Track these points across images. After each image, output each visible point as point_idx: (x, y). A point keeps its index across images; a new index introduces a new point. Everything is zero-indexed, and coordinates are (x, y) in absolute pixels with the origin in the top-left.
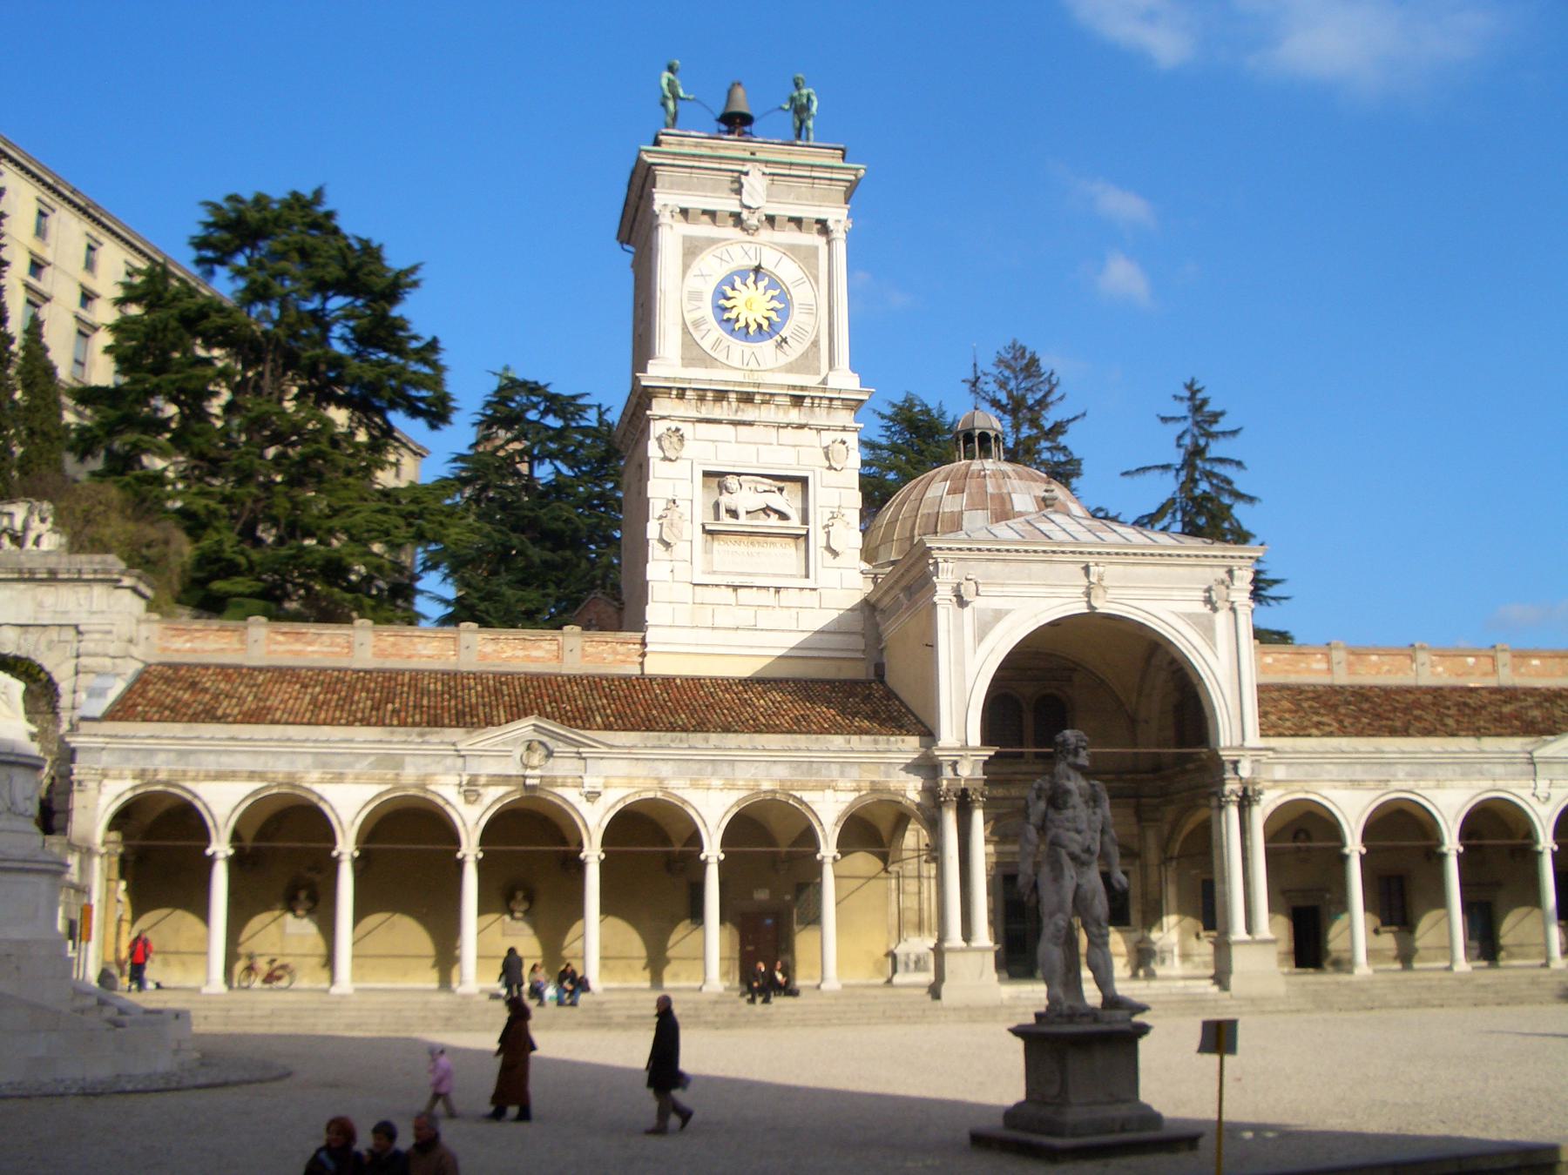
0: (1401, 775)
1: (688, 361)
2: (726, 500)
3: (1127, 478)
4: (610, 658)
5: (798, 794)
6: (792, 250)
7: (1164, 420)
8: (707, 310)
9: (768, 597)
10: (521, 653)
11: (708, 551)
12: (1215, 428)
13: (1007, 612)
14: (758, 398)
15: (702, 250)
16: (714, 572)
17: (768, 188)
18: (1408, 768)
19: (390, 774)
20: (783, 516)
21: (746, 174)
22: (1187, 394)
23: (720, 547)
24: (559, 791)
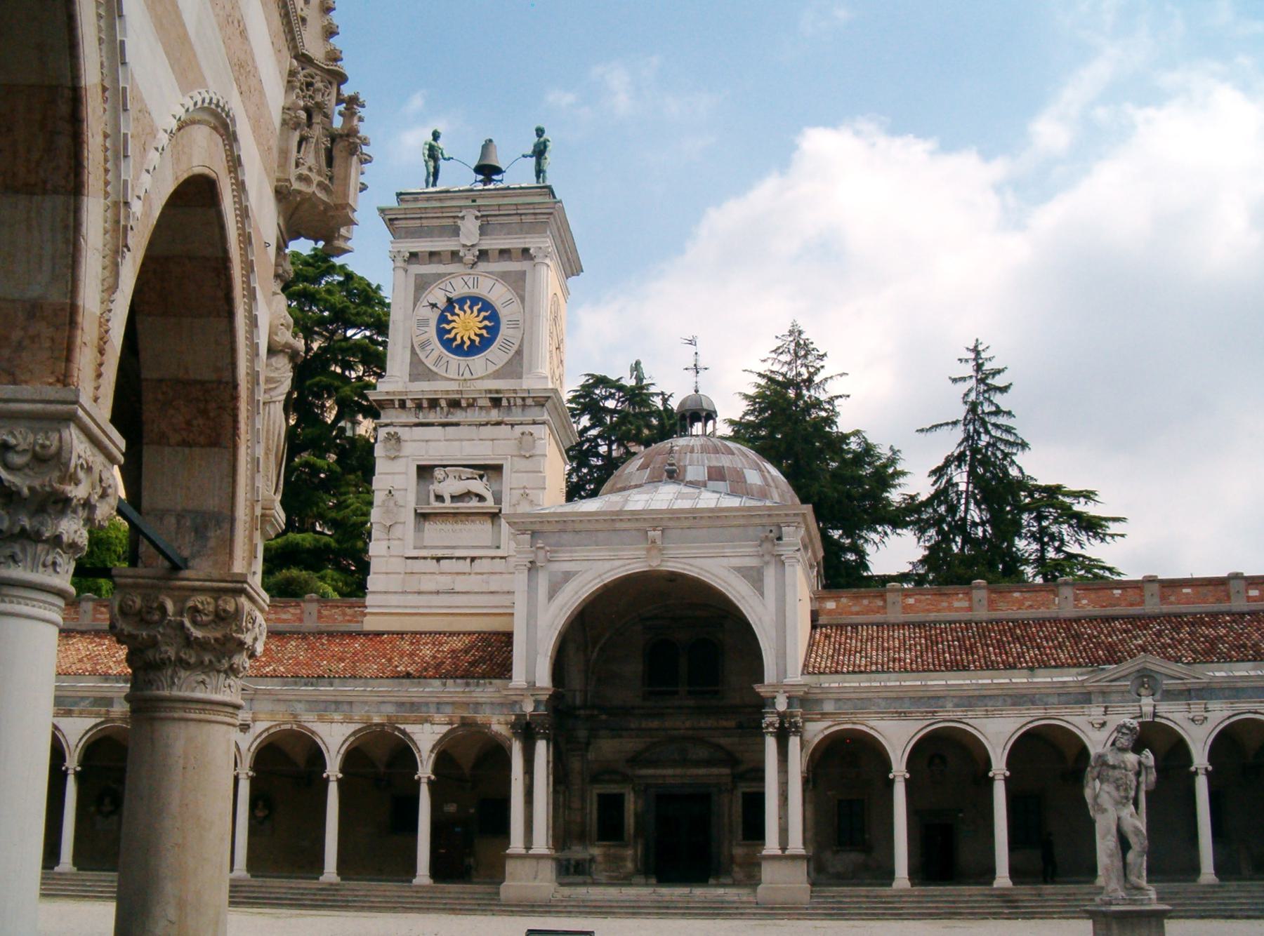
0: (949, 706)
1: (414, 377)
2: (436, 487)
3: (923, 435)
4: (340, 618)
5: (402, 727)
6: (504, 276)
7: (955, 380)
9: (464, 566)
11: (418, 529)
13: (576, 573)
14: (464, 404)
15: (430, 284)
16: (425, 547)
17: (481, 228)
18: (955, 700)
19: (103, 710)
20: (481, 498)
21: (463, 218)
22: (972, 355)
23: (429, 527)
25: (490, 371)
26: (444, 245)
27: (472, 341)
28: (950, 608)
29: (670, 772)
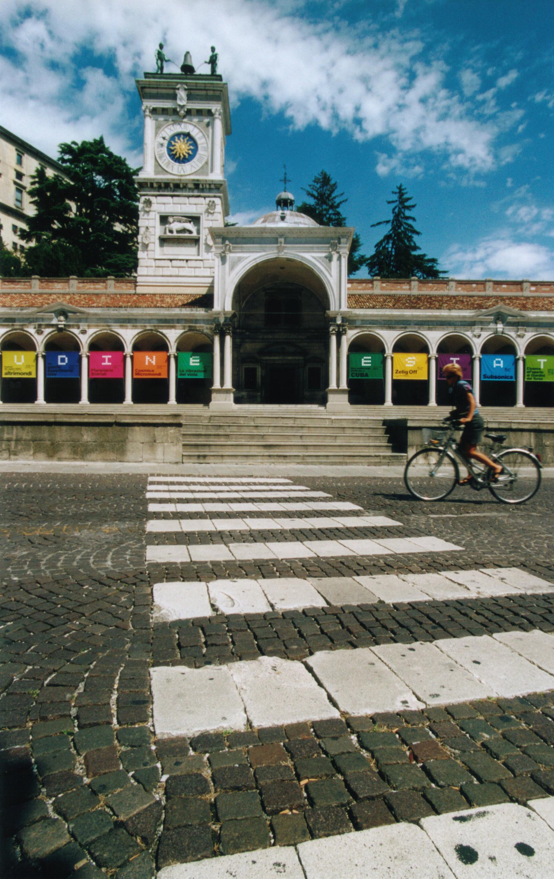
1: (156, 173)
3: (373, 228)
7: (389, 203)
8: (165, 150)
9: (183, 264)
10: (92, 287)
12: (407, 204)
13: (243, 258)
14: (181, 186)
16: (164, 255)
20: (190, 232)
24: (72, 330)
25: (193, 171)
26: (167, 104)
27: (184, 156)
28: (401, 289)
29: (277, 358)
